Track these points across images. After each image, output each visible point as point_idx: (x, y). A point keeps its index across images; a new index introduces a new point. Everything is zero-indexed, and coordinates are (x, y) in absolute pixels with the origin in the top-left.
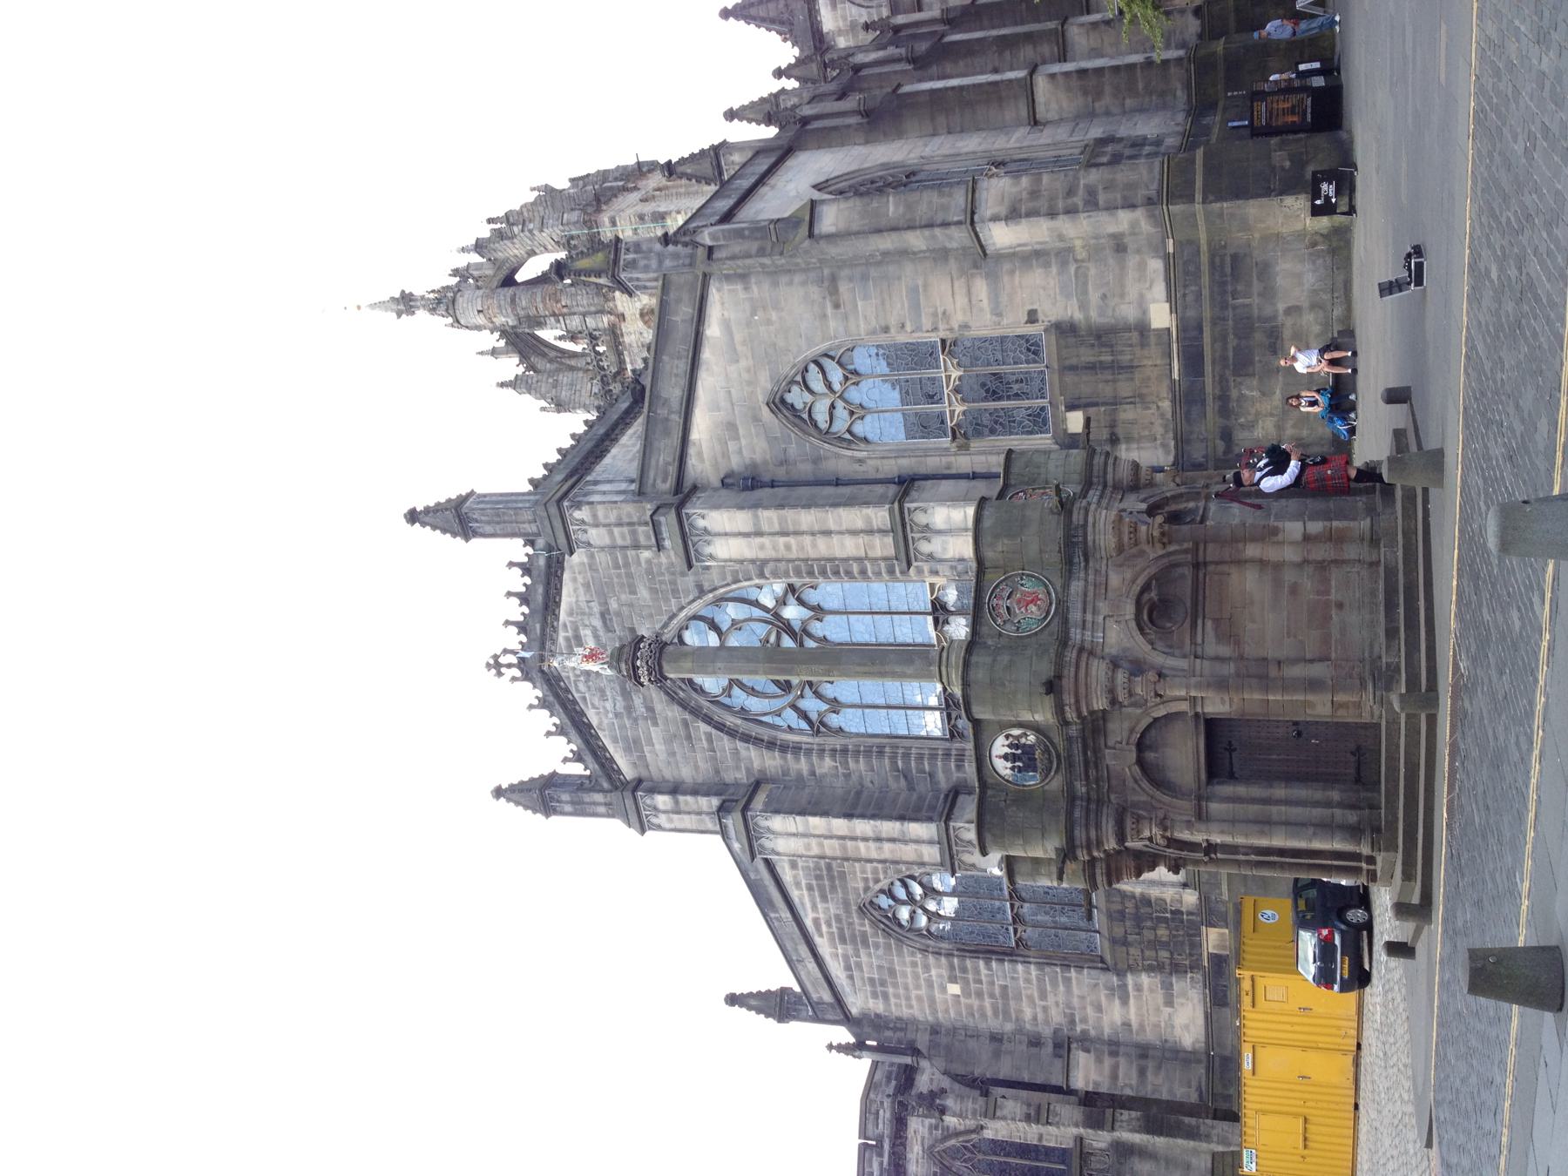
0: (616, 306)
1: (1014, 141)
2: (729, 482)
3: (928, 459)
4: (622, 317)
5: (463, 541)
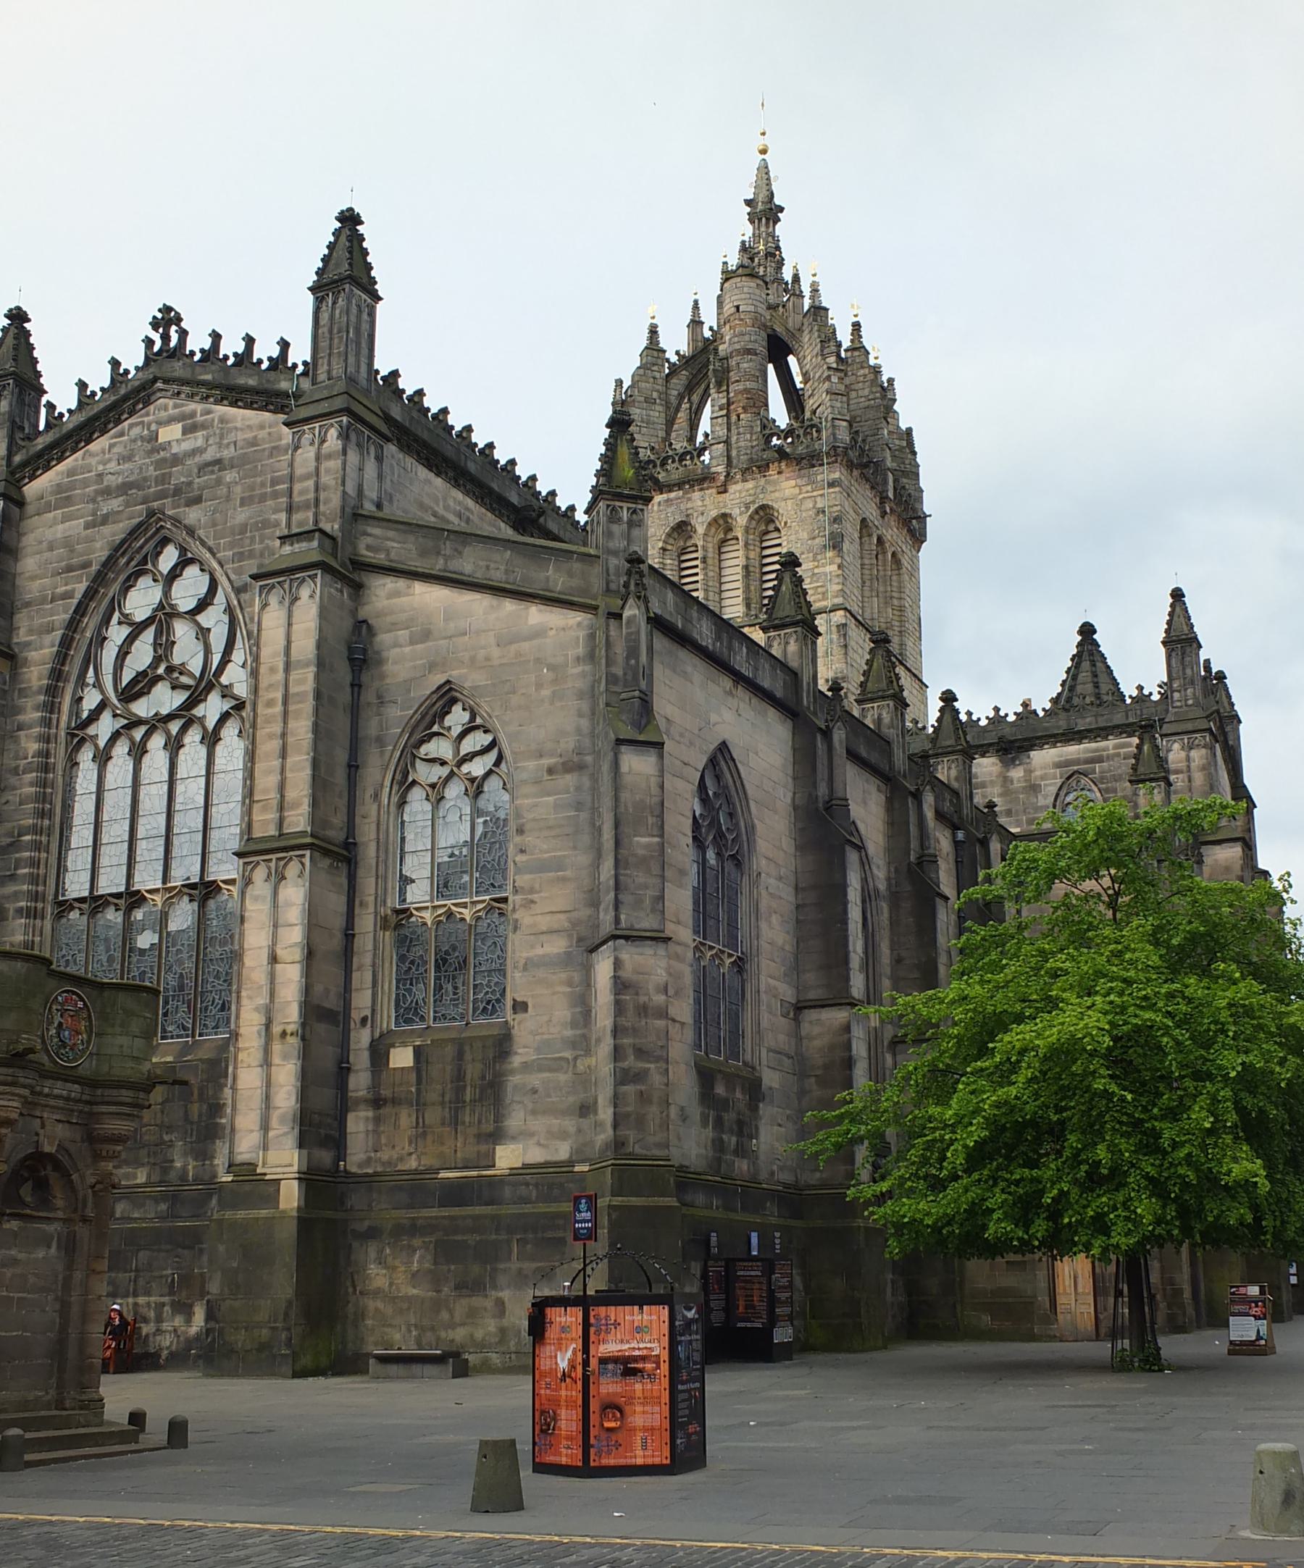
0: (735, 483)
2: (362, 630)
3: (373, 880)
4: (723, 490)
5: (311, 284)
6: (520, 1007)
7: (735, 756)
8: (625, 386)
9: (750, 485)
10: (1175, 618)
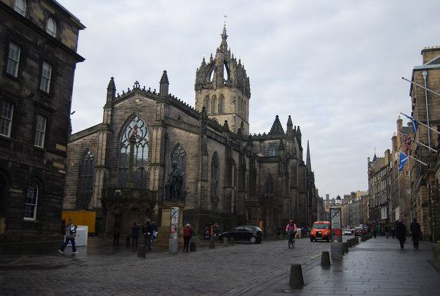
1: (221, 184)
6: (188, 188)
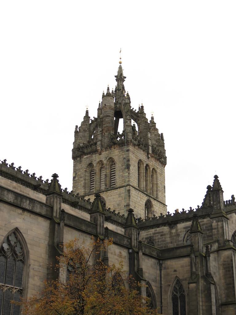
0: (103, 152)
4: (100, 154)
7: (21, 231)
8: (78, 127)
9: (107, 152)
10: (215, 184)
